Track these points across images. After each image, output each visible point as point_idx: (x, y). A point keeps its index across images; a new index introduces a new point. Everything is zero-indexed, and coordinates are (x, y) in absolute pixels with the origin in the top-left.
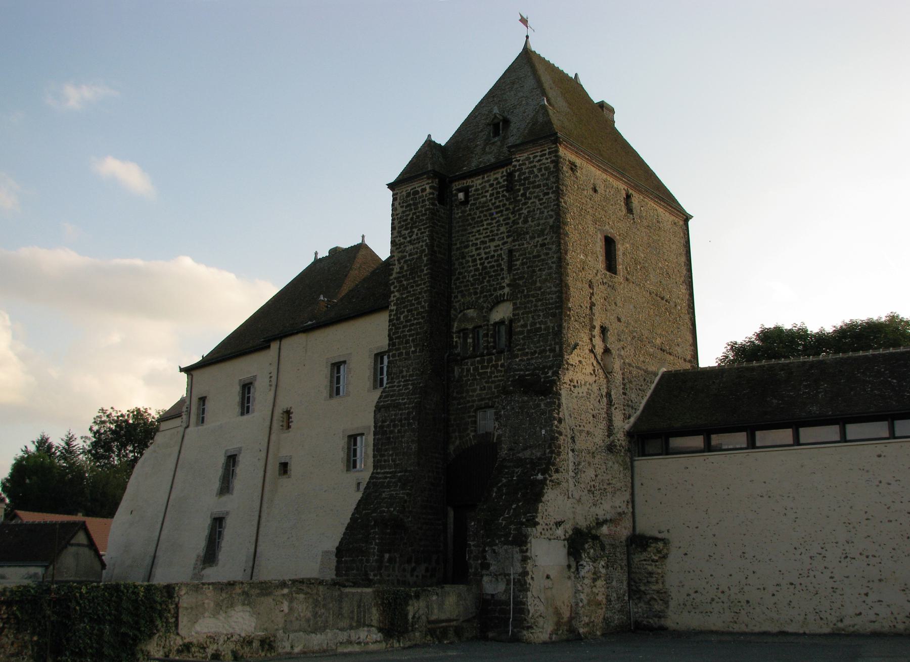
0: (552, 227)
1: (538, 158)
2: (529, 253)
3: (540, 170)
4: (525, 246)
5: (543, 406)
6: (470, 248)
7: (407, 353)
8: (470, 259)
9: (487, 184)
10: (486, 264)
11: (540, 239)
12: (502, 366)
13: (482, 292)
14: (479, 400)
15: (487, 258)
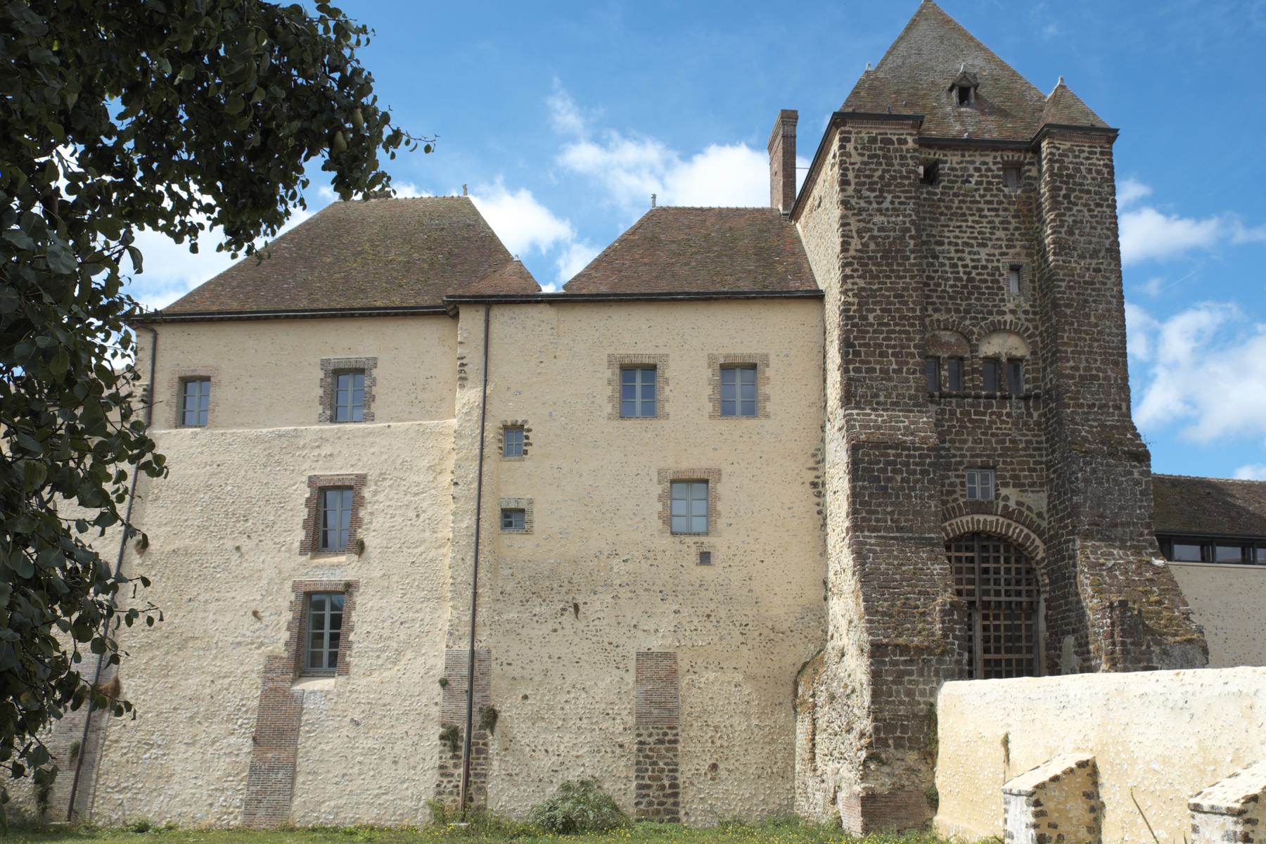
0: (1108, 250)
1: (1086, 154)
2: (1079, 275)
3: (1090, 171)
4: (1073, 265)
5: (1136, 475)
6: (946, 247)
7: (885, 372)
8: (947, 262)
9: (971, 167)
10: (973, 275)
11: (1094, 262)
12: (1009, 415)
13: (967, 312)
14: (972, 456)
15: (975, 267)
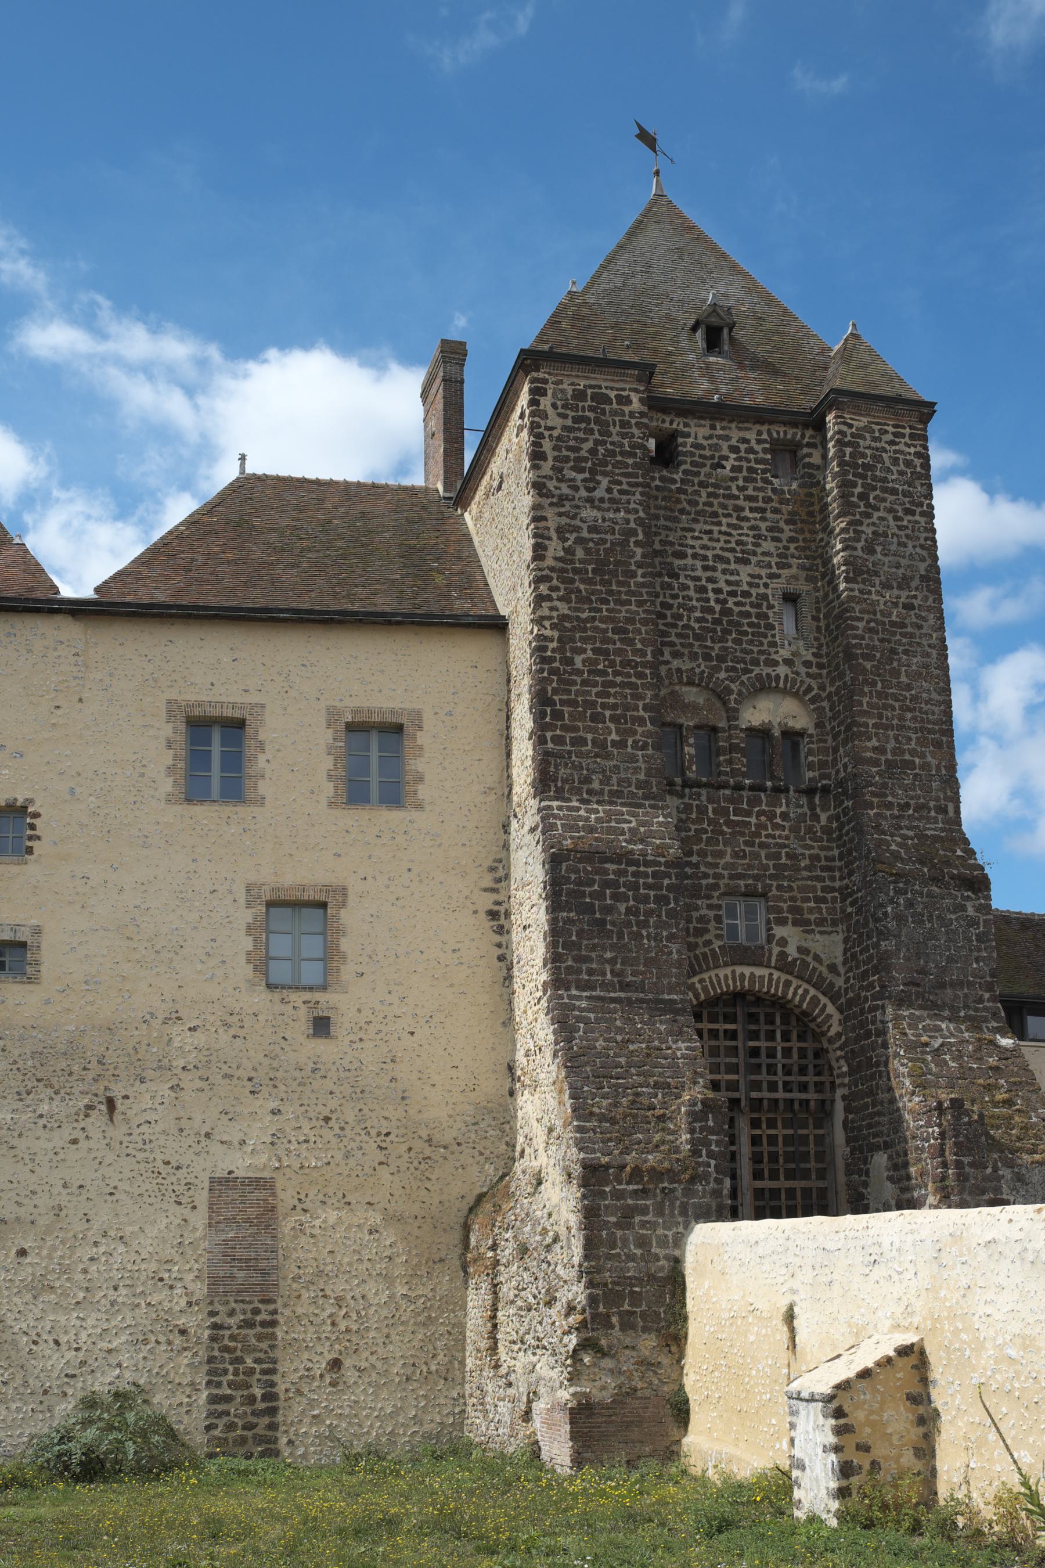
0: (923, 578)
1: (890, 437)
3: (895, 461)
4: (874, 597)
5: (970, 911)
6: (689, 561)
11: (904, 594)
12: (784, 816)
13: (721, 659)
14: (732, 877)
